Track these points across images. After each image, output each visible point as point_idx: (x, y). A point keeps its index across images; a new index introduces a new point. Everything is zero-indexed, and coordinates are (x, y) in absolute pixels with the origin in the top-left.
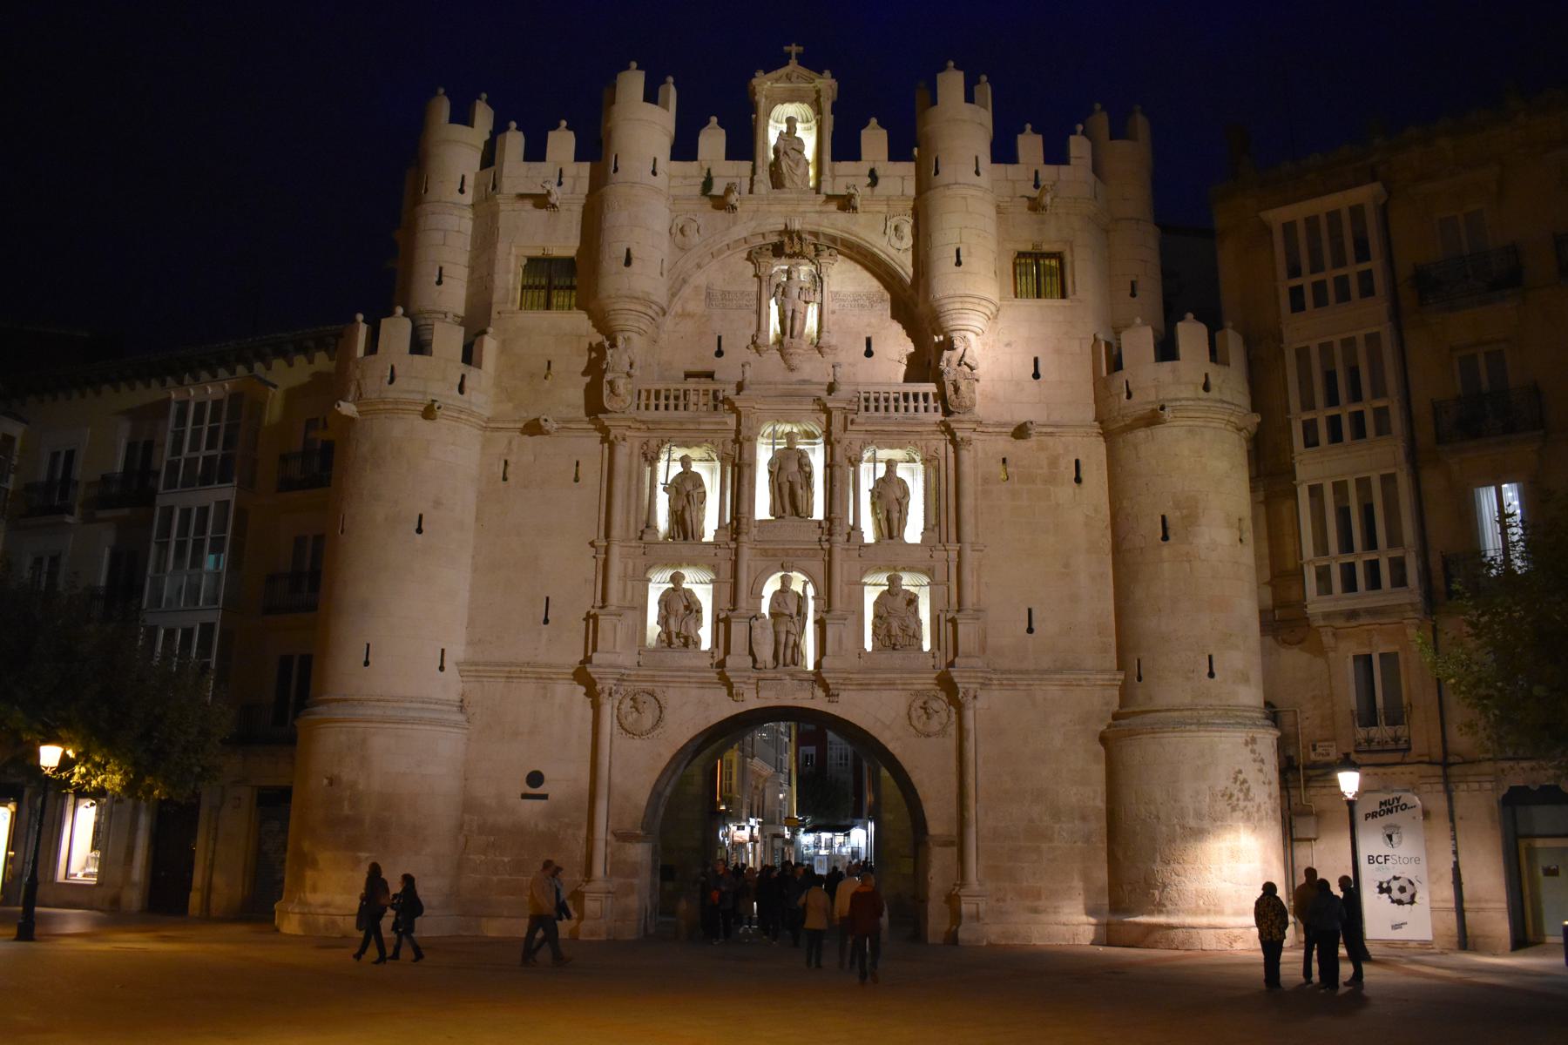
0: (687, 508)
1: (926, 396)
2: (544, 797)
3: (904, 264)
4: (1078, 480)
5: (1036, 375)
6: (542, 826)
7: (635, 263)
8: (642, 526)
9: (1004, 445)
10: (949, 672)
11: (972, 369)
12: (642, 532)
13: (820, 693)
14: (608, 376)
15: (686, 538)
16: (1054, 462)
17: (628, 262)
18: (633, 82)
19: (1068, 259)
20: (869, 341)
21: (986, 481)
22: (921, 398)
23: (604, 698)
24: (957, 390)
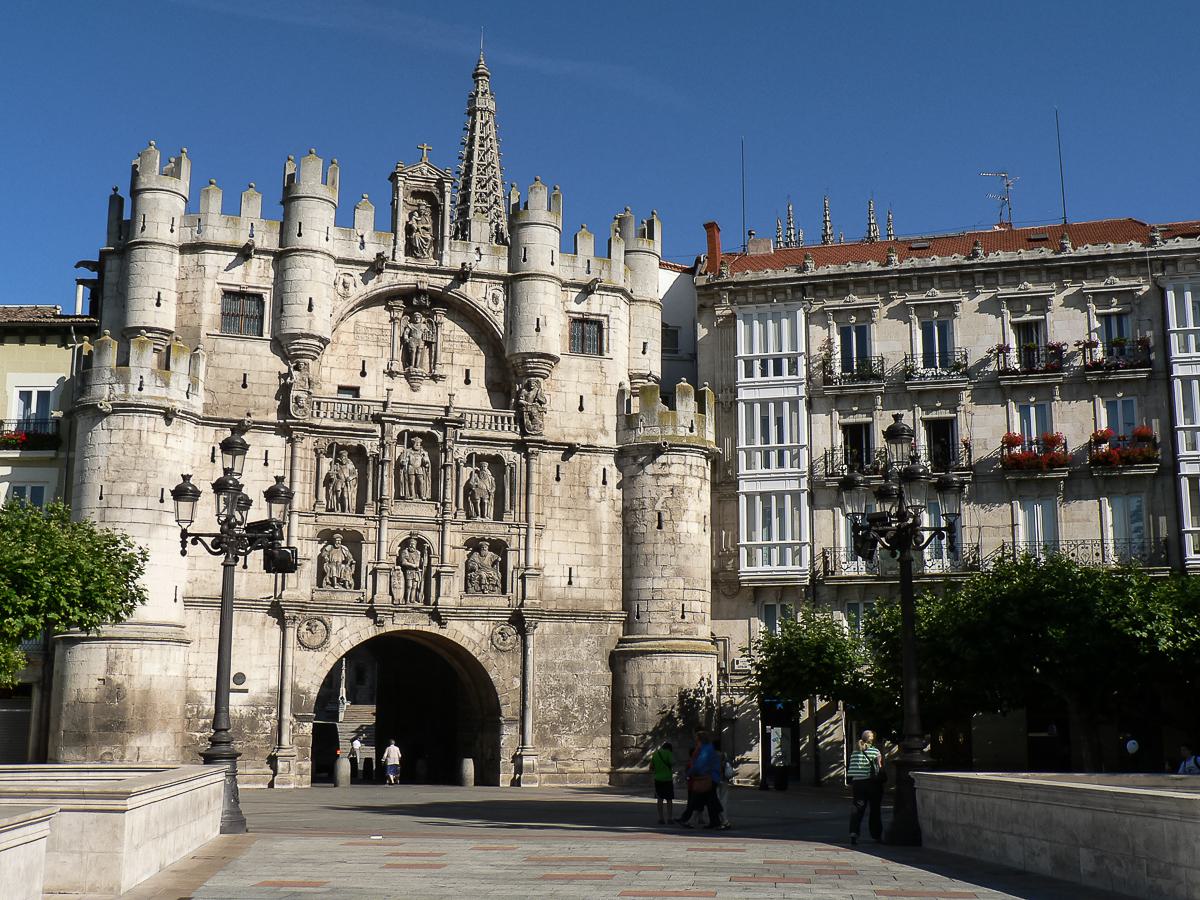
0: (345, 490)
1: (509, 419)
2: (246, 691)
3: (499, 321)
5: (581, 409)
6: (245, 711)
7: (315, 308)
8: (314, 501)
10: (520, 610)
11: (541, 403)
12: (314, 506)
14: (294, 394)
15: (343, 510)
17: (310, 309)
19: (605, 326)
20: (467, 371)
22: (506, 421)
23: (288, 624)
24: (531, 418)
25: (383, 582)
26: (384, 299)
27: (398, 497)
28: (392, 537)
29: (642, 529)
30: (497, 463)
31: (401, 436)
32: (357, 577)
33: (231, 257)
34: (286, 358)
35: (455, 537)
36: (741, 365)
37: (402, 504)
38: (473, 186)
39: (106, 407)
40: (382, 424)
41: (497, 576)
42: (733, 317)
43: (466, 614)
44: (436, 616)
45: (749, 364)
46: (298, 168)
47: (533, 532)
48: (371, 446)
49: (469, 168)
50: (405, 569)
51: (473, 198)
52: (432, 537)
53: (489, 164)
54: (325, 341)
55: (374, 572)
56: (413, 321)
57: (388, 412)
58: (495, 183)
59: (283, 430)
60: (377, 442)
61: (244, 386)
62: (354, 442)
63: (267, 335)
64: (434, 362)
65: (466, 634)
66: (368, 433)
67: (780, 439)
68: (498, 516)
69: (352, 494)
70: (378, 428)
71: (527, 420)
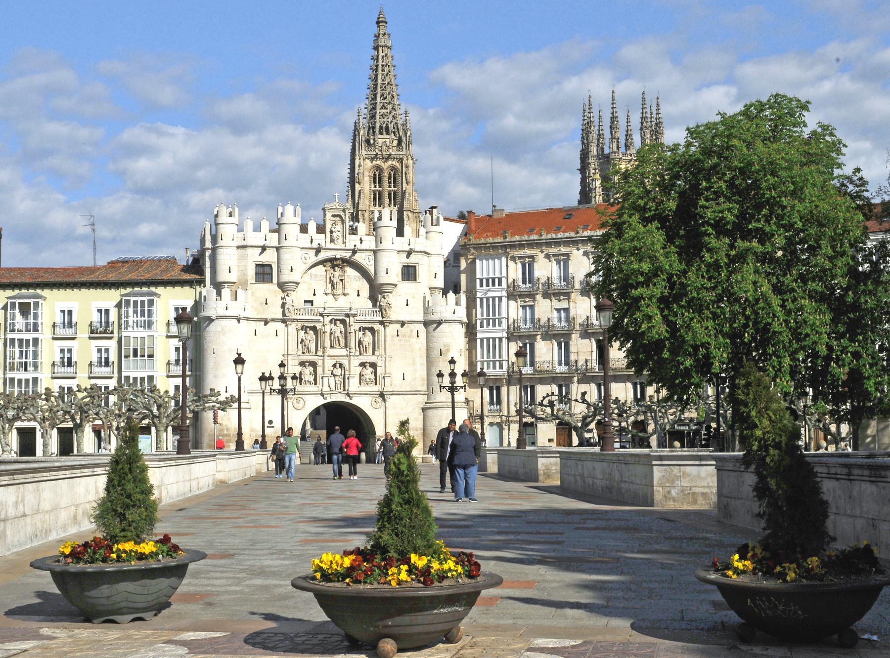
4: (418, 336)
5: (407, 305)
9: (398, 326)
13: (348, 398)
14: (287, 307)
16: (411, 331)
17: (292, 270)
18: (289, 209)
21: (392, 337)
25: (326, 380)
26: (323, 262)
27: (332, 347)
28: (329, 363)
29: (434, 356)
30: (372, 330)
31: (331, 321)
32: (315, 380)
33: (260, 250)
34: (283, 291)
35: (355, 362)
36: (478, 281)
37: (332, 349)
38: (378, 99)
39: (214, 317)
40: (323, 316)
41: (373, 377)
42: (474, 261)
43: (360, 394)
44: (348, 395)
45: (481, 281)
46: (284, 209)
47: (388, 358)
48: (319, 326)
49: (376, 85)
50: (335, 376)
51: (379, 106)
52: (345, 363)
53: (388, 83)
54: (298, 283)
55: (322, 378)
56: (334, 271)
57: (326, 312)
58: (392, 95)
59: (283, 321)
60: (321, 324)
61: (266, 304)
62: (312, 324)
63: (275, 281)
64: (344, 288)
65: (363, 403)
66: (318, 321)
67: (494, 314)
68: (373, 353)
69: (312, 347)
70: (321, 318)
71: (384, 312)
